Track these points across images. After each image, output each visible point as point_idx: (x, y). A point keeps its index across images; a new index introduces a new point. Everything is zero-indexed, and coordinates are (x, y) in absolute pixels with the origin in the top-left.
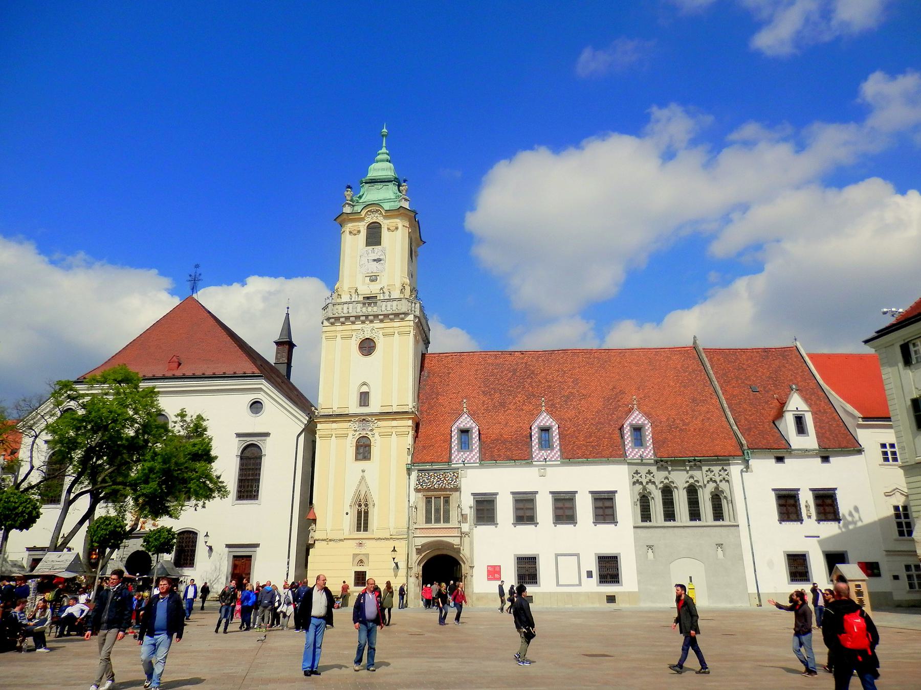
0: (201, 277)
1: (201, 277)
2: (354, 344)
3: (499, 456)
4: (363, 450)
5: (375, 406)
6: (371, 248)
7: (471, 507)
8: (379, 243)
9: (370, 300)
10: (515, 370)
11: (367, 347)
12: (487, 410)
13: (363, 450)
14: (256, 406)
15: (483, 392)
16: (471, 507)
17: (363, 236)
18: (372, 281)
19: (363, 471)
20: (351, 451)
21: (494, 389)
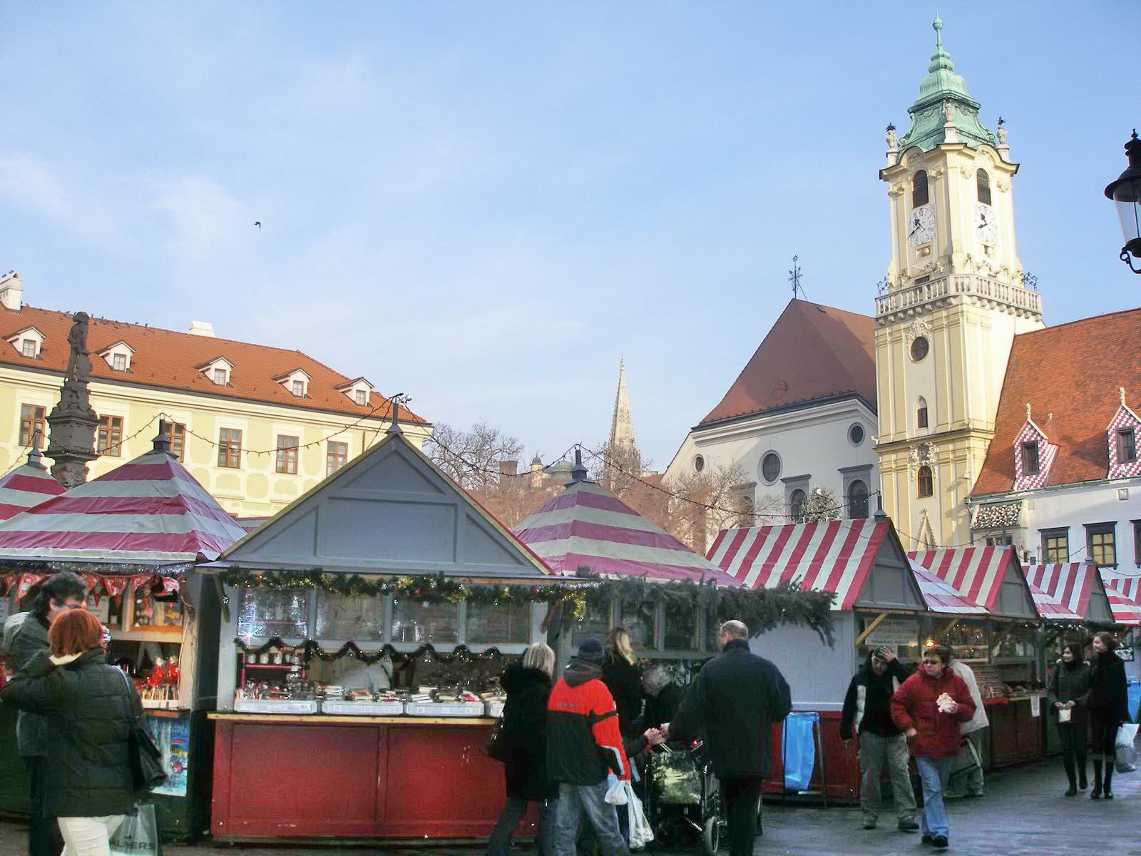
0: (801, 272)
1: (801, 272)
2: (906, 348)
3: (1072, 475)
4: (926, 484)
5: (931, 429)
6: (918, 209)
7: (1038, 548)
8: (927, 201)
9: (922, 280)
10: (1124, 342)
11: (920, 348)
12: (1077, 410)
13: (926, 484)
14: (857, 434)
15: (1077, 383)
16: (1038, 548)
17: (907, 197)
18: (924, 255)
19: (924, 511)
20: (913, 486)
21: (1091, 376)
